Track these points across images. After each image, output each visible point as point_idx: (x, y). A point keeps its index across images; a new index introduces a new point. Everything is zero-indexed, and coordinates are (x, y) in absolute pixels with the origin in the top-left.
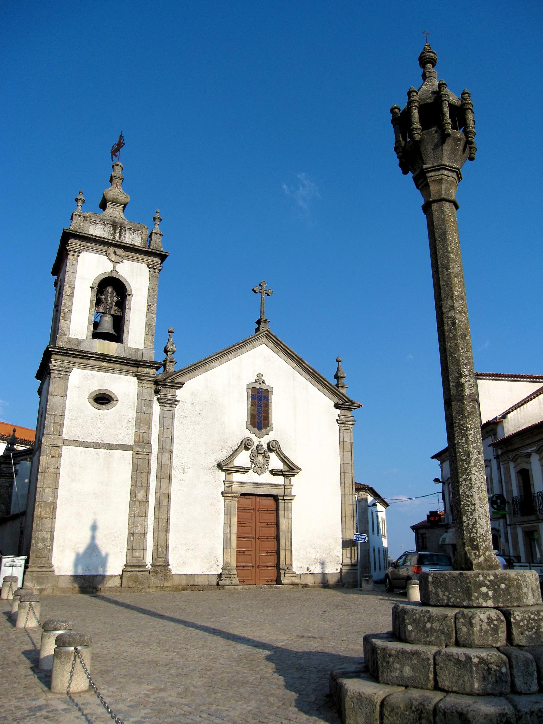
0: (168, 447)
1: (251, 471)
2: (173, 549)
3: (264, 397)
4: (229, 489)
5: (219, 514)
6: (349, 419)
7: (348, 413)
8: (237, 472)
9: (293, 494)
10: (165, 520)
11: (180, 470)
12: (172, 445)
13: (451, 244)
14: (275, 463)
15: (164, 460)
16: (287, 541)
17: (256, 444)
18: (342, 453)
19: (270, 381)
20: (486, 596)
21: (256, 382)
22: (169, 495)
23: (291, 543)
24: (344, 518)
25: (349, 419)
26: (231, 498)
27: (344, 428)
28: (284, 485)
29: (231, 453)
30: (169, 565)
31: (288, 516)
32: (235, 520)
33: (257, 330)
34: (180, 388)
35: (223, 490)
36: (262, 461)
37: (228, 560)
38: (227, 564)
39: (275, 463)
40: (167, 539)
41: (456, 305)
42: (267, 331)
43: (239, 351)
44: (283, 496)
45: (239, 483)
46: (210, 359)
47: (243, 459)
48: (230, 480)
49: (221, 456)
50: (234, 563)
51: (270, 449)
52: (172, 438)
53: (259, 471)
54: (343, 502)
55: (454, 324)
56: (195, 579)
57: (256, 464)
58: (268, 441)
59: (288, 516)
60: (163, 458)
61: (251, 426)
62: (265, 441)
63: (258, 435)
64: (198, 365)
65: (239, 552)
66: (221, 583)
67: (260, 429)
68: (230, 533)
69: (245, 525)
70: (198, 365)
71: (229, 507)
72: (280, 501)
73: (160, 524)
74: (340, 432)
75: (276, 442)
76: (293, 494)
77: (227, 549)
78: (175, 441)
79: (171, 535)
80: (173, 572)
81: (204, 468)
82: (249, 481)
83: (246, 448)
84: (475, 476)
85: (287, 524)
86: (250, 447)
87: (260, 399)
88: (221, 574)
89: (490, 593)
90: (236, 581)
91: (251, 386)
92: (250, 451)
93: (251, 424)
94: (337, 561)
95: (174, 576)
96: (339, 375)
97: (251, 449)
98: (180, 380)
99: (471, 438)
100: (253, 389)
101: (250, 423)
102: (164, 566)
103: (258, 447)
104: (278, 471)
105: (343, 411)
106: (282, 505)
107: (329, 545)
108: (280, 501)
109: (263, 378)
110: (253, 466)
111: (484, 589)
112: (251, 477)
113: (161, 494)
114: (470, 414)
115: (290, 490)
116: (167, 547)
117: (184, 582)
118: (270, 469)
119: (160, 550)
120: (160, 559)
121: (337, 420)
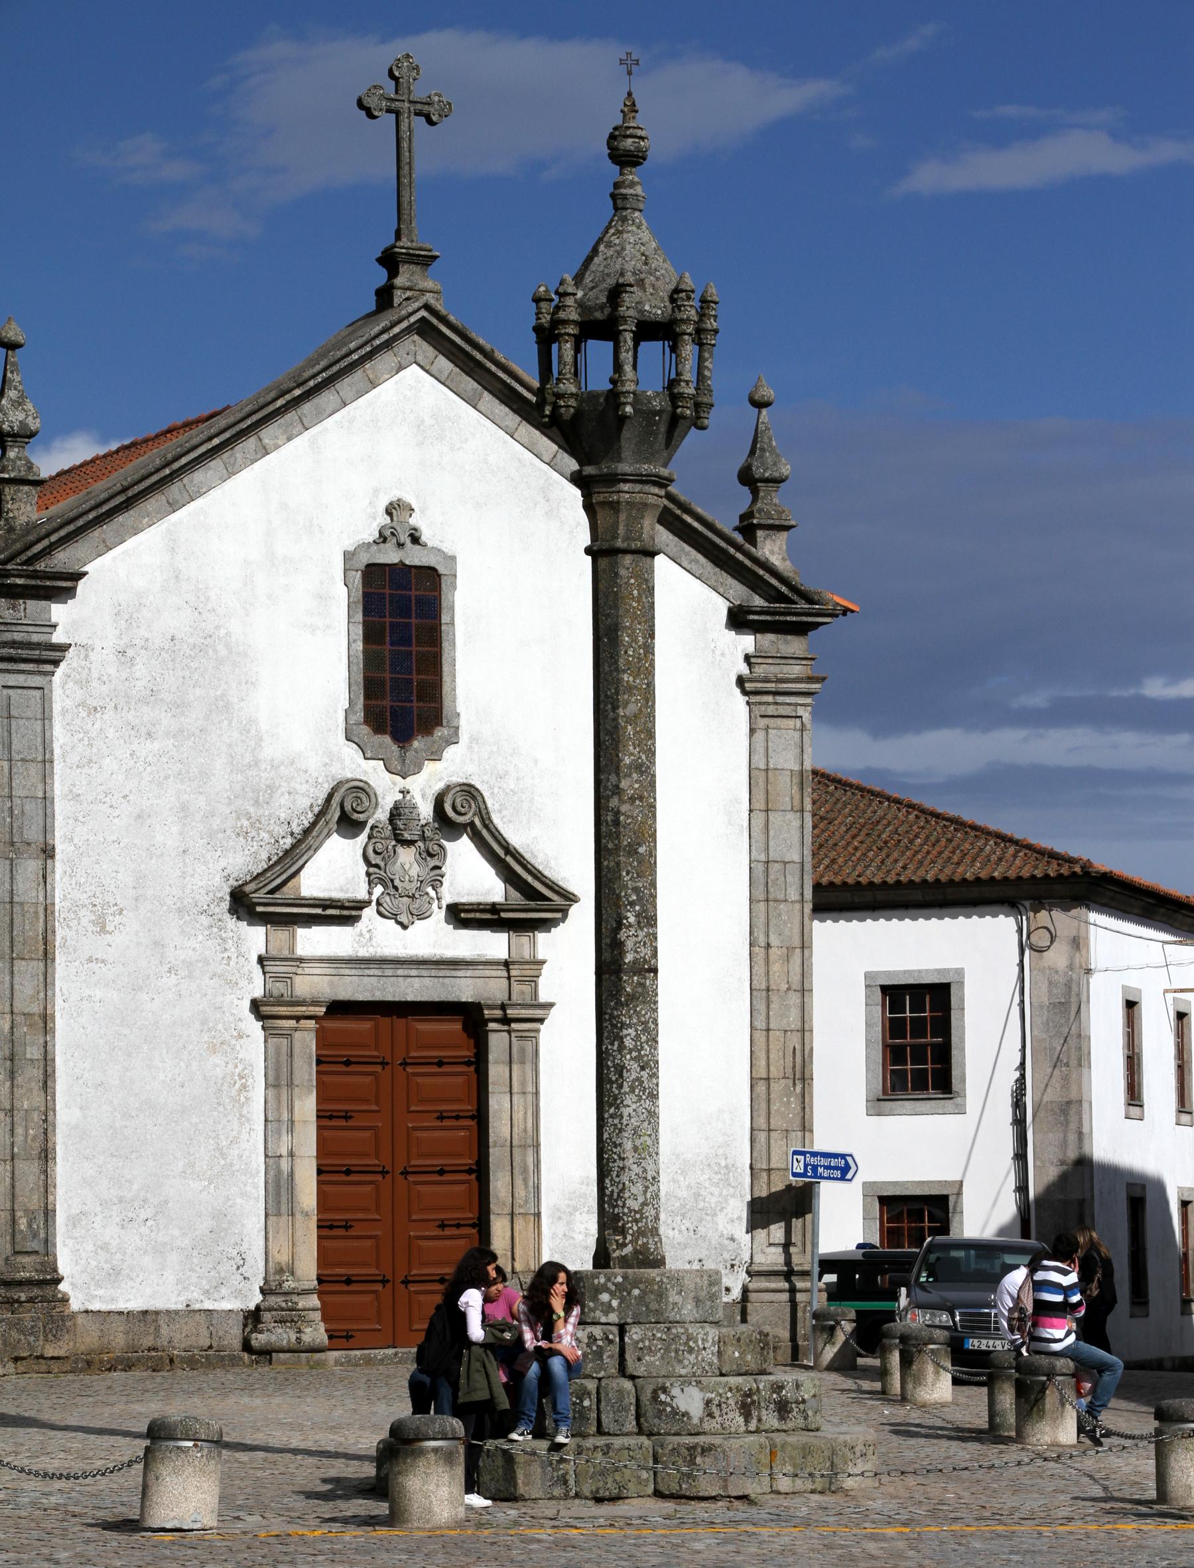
0: (33, 833)
1: (369, 913)
2: (74, 1221)
3: (419, 600)
4: (279, 988)
5: (244, 1087)
6: (796, 670)
7: (794, 645)
8: (310, 921)
9: (543, 997)
10: (35, 1116)
11: (84, 922)
12: (47, 829)
13: (626, 652)
14: (469, 875)
15: (20, 886)
16: (519, 1181)
17: (387, 801)
18: (759, 818)
19: (443, 530)
20: (608, 1309)
21: (383, 538)
22: (45, 1022)
23: (537, 1189)
24: (761, 1088)
25: (796, 670)
26: (292, 1023)
27: (771, 710)
28: (506, 964)
29: (288, 842)
30: (59, 1281)
31: (523, 1083)
32: (307, 1106)
33: (384, 297)
34: (70, 593)
35: (258, 993)
36: (415, 870)
37: (284, 1258)
38: (280, 1271)
39: (469, 875)
40: (47, 1186)
41: (624, 784)
42: (427, 307)
43: (307, 408)
44: (503, 1007)
45: (321, 960)
46: (184, 461)
47: (334, 868)
48: (285, 953)
49: (244, 860)
50: (308, 1269)
51: (446, 823)
52: (47, 800)
53: (404, 908)
54: (760, 1024)
55: (617, 823)
56: (157, 1329)
57: (390, 884)
58: (439, 786)
59: (523, 1083)
60: (19, 878)
61: (365, 729)
62: (423, 787)
63: (396, 765)
64: (137, 489)
65: (329, 1227)
66: (259, 1340)
67: (402, 737)
68: (291, 1154)
69: (351, 1123)
70: (137, 489)
71: (284, 1058)
72: (492, 1026)
73: (19, 1131)
74: (752, 731)
75: (470, 792)
76: (543, 997)
77: (279, 1214)
78: (61, 808)
79: (62, 1168)
80: (75, 1305)
81: (179, 911)
82: (363, 953)
83: (349, 825)
84: (630, 1110)
85: (519, 1116)
86: (362, 817)
87: (403, 608)
88: (258, 1308)
89: (615, 1303)
90: (316, 1333)
91: (364, 559)
92: (363, 837)
93: (367, 721)
94: (726, 1256)
95: (80, 1320)
96: (758, 472)
97: (370, 823)
98: (62, 559)
99: (628, 1042)
100: (372, 572)
101: (360, 715)
102: (41, 1283)
103: (396, 813)
104: (478, 907)
105: (768, 639)
106: (497, 1042)
107: (697, 1196)
108: (492, 1026)
109: (413, 521)
110: (378, 890)
111: (605, 1297)
112: (377, 935)
113: (19, 1019)
114: (632, 997)
115: (533, 980)
116: (48, 1213)
117: (119, 1340)
118: (448, 899)
119: (23, 1224)
120: (26, 1260)
121: (741, 681)
